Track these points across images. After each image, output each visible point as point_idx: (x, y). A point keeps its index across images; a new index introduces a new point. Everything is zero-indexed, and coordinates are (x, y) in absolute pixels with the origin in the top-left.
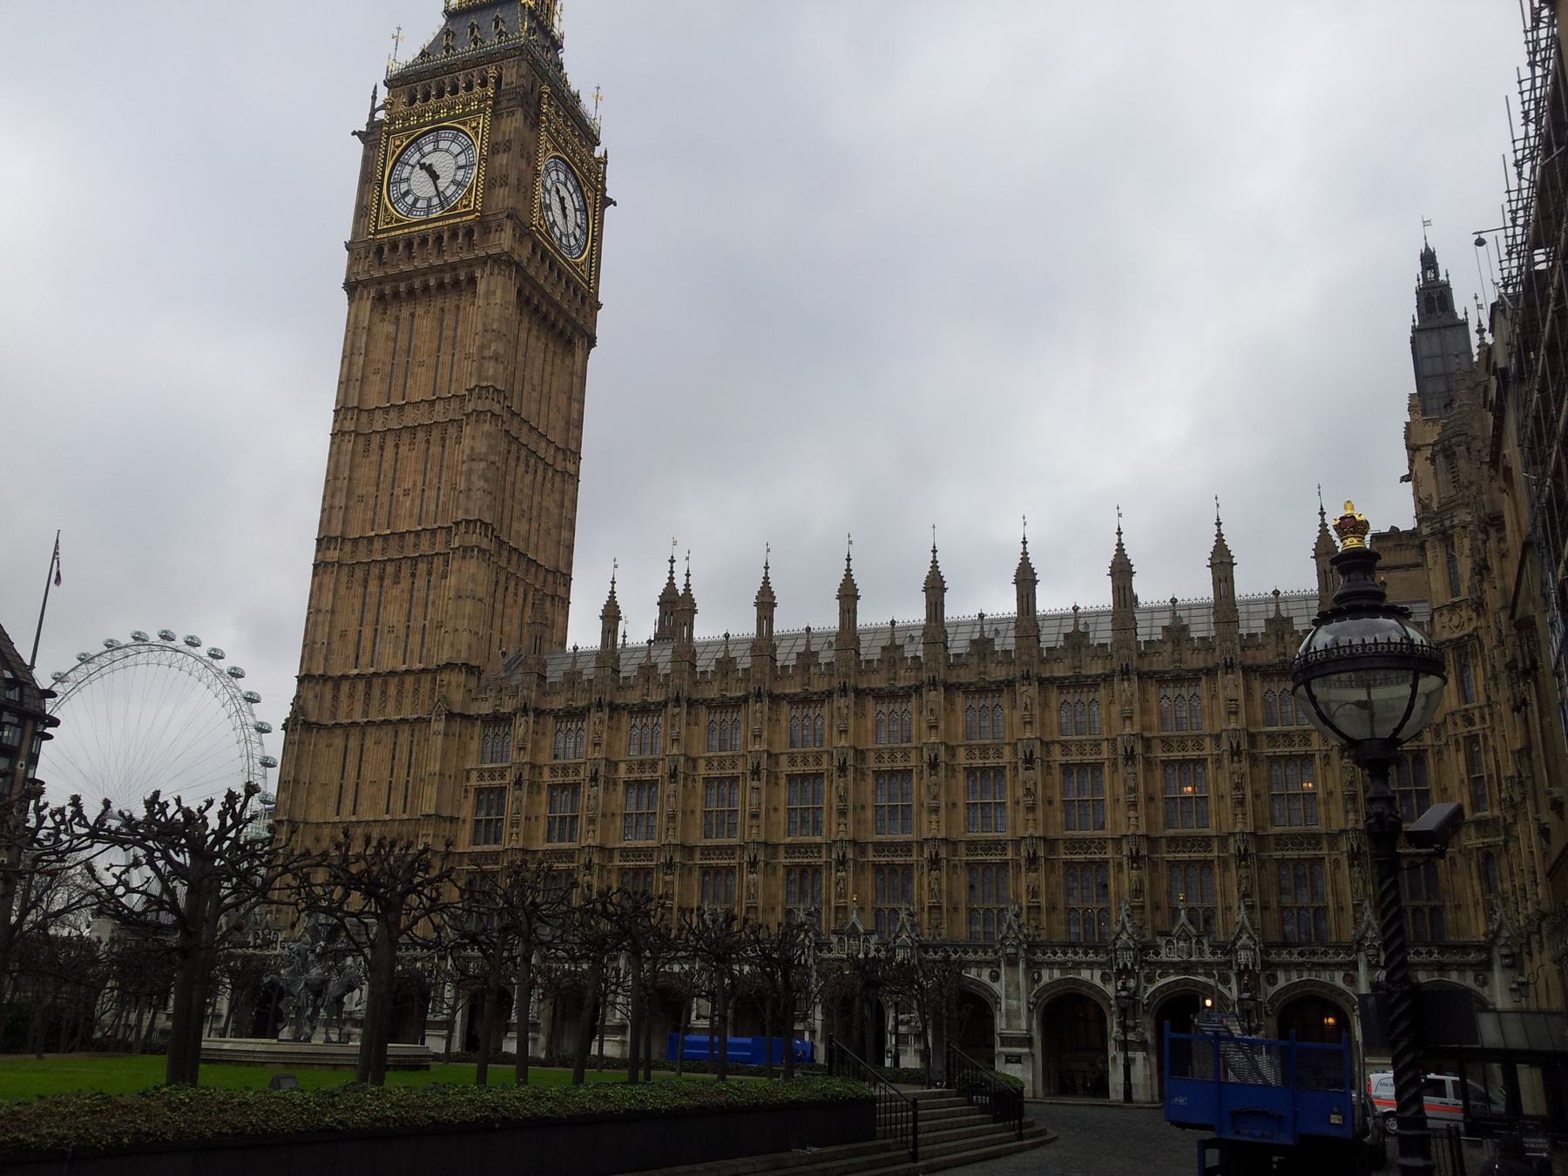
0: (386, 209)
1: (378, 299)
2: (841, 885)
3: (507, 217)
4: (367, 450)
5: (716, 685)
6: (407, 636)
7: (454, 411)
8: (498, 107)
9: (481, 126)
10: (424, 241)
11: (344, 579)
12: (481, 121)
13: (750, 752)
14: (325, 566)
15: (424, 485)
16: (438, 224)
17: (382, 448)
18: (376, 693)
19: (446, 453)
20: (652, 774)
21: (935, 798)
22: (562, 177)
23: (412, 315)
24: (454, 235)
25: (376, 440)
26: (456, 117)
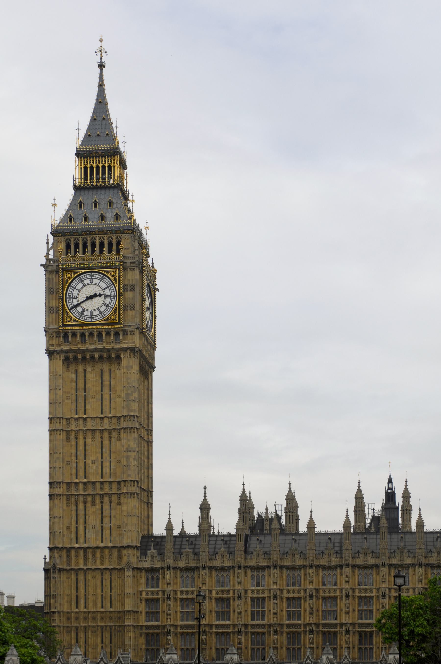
0: (67, 313)
1: (65, 360)
2: (312, 639)
3: (137, 328)
4: (68, 439)
5: (254, 560)
6: (102, 530)
7: (114, 424)
8: (125, 265)
9: (117, 275)
10: (91, 334)
11: (65, 502)
12: (117, 272)
13: (272, 589)
14: (56, 496)
15: (102, 458)
16: (99, 327)
17: (76, 438)
18: (90, 556)
20: (227, 595)
21: (348, 608)
23: (85, 370)
24: (108, 333)
25: (73, 434)
26: (101, 267)
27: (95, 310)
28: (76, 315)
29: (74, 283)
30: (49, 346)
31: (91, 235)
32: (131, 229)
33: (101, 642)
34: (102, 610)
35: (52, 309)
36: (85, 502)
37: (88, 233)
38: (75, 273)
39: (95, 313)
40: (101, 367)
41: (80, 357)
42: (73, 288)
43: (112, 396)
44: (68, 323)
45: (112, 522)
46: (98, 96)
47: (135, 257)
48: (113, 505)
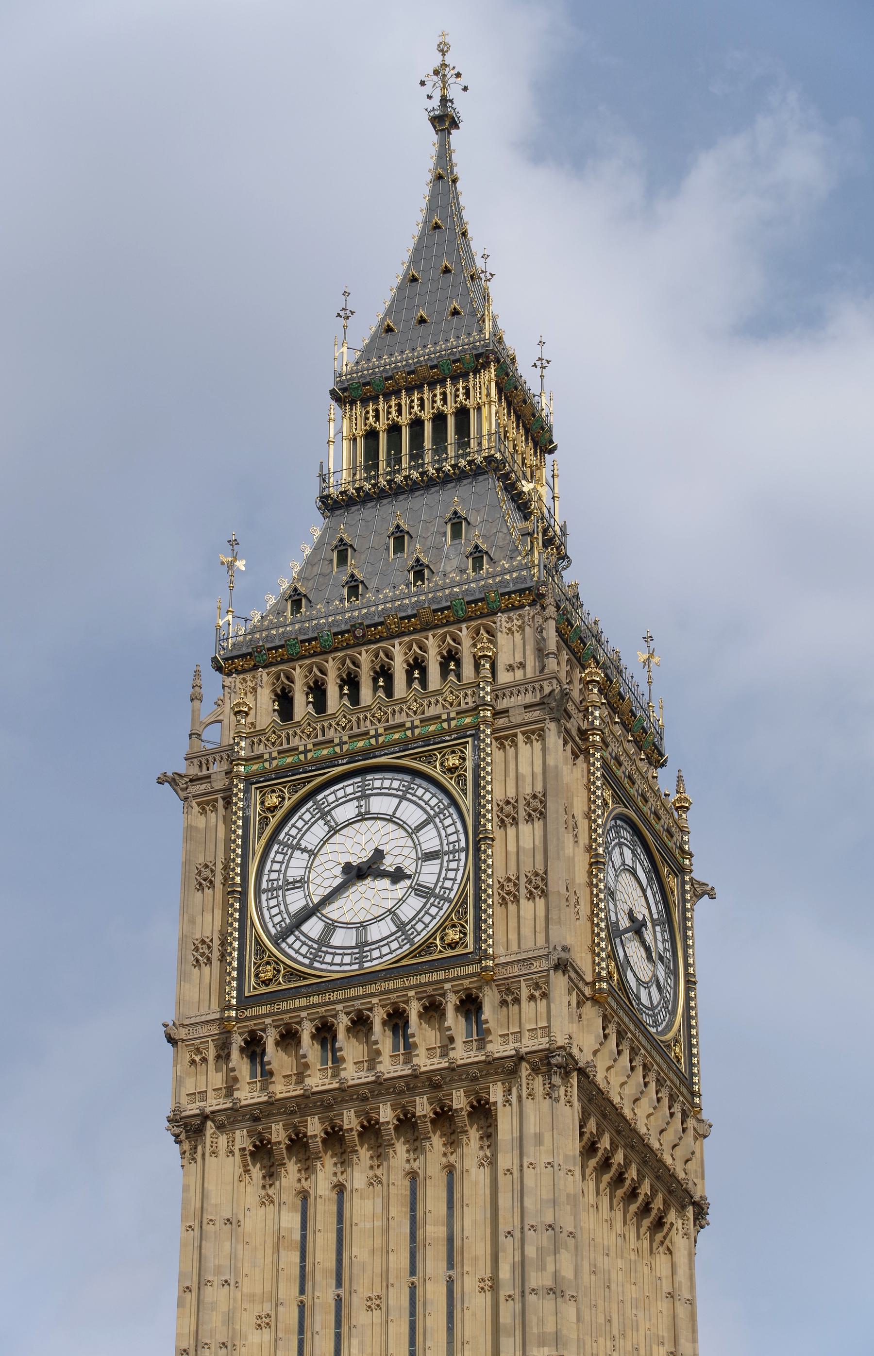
1: (252, 1154)
3: (556, 967)
8: (501, 722)
9: (469, 764)
12: (469, 752)
27: (377, 919)
28: (297, 952)
29: (293, 826)
30: (184, 1100)
31: (371, 642)
32: (529, 584)
37: (359, 633)
39: (375, 932)
40: (407, 1166)
44: (263, 990)
47: (545, 684)
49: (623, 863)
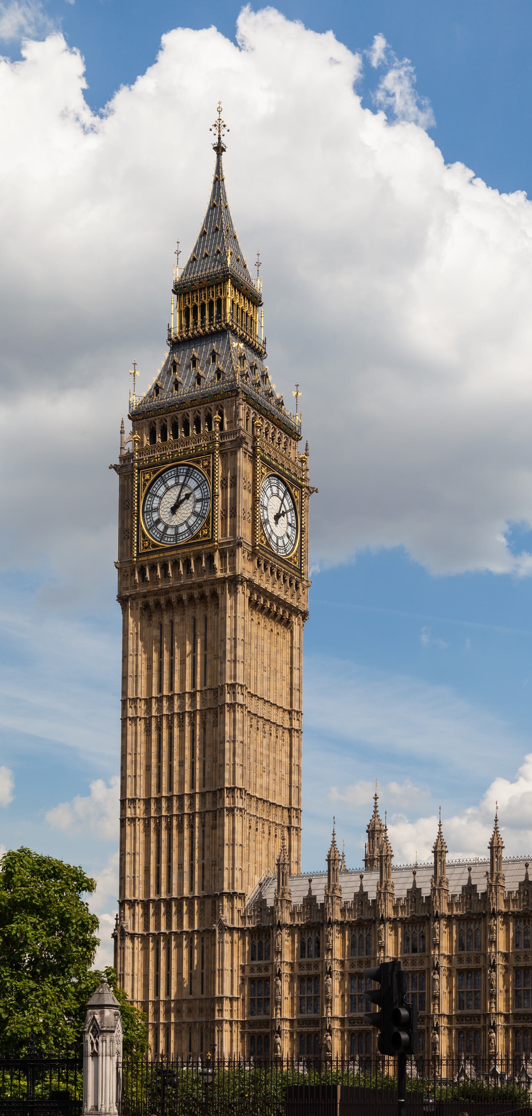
0: (144, 535)
4: (148, 731)
19: (208, 733)
22: (275, 489)
23: (172, 622)
33: (188, 1049)
34: (191, 997)
35: (126, 533)
36: (169, 828)
38: (154, 473)
41: (163, 601)
42: (154, 495)
43: (209, 657)
45: (206, 857)
46: (213, 195)
48: (207, 829)
49: (272, 493)
